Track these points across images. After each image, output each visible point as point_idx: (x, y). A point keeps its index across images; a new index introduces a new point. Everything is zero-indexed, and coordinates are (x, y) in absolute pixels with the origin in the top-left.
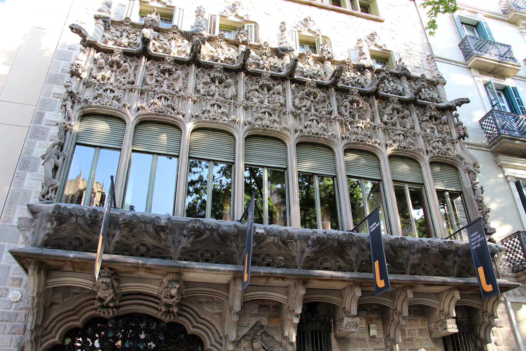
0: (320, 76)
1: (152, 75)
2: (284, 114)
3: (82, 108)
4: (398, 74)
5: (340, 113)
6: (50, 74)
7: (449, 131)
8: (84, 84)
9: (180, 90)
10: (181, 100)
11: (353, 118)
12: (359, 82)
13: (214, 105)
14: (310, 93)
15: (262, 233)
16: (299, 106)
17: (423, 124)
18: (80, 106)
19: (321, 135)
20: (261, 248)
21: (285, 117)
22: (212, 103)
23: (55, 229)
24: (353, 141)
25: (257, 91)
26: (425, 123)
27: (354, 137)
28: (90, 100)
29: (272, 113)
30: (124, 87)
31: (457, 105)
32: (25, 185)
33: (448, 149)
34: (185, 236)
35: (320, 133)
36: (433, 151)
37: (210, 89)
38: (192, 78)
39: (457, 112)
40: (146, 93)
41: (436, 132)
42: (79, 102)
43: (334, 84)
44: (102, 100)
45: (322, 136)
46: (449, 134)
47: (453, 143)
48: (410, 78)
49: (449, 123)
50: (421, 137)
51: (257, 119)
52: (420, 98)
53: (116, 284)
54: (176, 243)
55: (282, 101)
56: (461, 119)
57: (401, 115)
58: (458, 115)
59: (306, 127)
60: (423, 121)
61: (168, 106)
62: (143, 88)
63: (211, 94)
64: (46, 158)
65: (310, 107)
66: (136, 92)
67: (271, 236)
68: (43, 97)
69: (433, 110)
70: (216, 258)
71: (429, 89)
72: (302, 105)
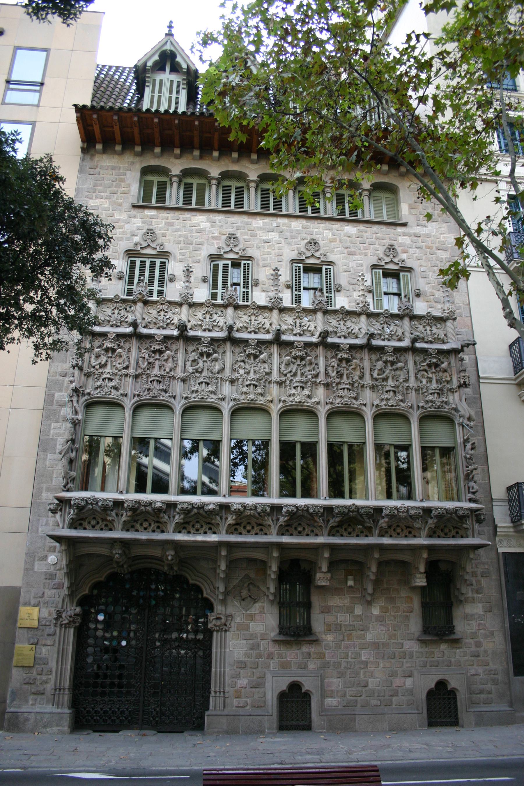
0: (310, 331)
1: (144, 358)
3: (86, 400)
5: (327, 374)
8: (85, 375)
9: (171, 370)
12: (353, 332)
16: (285, 373)
19: (304, 402)
20: (241, 519)
22: (200, 381)
23: (76, 514)
24: (337, 405)
25: (243, 361)
27: (338, 400)
30: (120, 373)
41: (434, 381)
50: (413, 391)
53: (127, 551)
54: (172, 518)
55: (267, 370)
60: (420, 370)
62: (137, 373)
63: (200, 370)
64: (63, 453)
70: (204, 528)
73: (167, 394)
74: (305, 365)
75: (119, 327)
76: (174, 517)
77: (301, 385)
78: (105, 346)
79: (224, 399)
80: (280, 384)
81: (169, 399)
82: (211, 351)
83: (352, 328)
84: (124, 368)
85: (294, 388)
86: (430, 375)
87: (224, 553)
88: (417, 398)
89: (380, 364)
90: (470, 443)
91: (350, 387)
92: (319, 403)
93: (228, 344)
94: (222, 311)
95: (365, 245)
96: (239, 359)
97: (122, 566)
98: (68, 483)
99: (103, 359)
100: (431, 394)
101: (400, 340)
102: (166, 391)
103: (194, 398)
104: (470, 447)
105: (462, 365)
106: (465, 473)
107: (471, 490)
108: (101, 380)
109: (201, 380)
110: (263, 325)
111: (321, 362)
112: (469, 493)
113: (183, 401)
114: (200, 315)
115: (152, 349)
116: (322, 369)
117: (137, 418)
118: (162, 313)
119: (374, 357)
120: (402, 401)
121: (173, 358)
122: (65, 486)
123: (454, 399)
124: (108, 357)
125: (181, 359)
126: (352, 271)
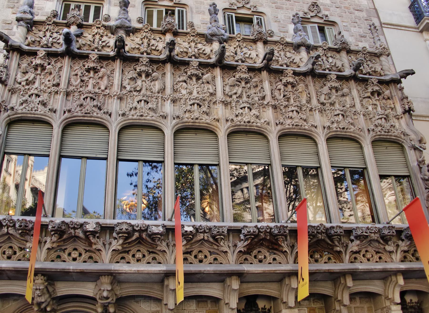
0: (252, 58)
1: (76, 75)
2: (214, 103)
3: (9, 116)
4: (336, 49)
5: (273, 98)
7: (393, 106)
8: (9, 91)
9: (106, 88)
10: (107, 98)
11: (288, 101)
12: (294, 61)
13: (141, 101)
14: (241, 79)
15: (191, 231)
16: (229, 94)
17: (365, 101)
18: (6, 114)
19: (253, 123)
21: (216, 107)
22: (138, 99)
24: (287, 126)
25: (185, 82)
26: (367, 99)
27: (289, 121)
28: (16, 108)
29: (201, 104)
30: (49, 90)
31: (402, 77)
33: (392, 125)
34: (115, 238)
35: (252, 121)
36: (375, 130)
37: (136, 85)
38: (117, 74)
39: (402, 85)
40: (72, 95)
41: (379, 108)
42: (5, 109)
43: (267, 68)
44: (28, 106)
45: (254, 124)
46: (394, 109)
47: (398, 119)
48: (349, 52)
49: (394, 97)
50: (362, 116)
51: (185, 112)
52: (362, 73)
54: (107, 246)
55: (211, 91)
56: (406, 92)
57: (340, 93)
58: (403, 88)
60: (364, 98)
61: (94, 106)
62: (68, 90)
63: (138, 89)
65: (242, 94)
66: (62, 94)
69: (375, 85)
70: (147, 258)
71: (371, 62)
72: (233, 92)
73: (102, 111)
74: (250, 88)
76: (110, 244)
77: (248, 106)
78: (34, 64)
79: (165, 117)
80: (226, 104)
84: (54, 85)
86: (375, 102)
91: (299, 110)
93: (168, 66)
94: (160, 38)
95: (290, 2)
99: (30, 76)
102: (100, 109)
103: (133, 116)
105: (403, 94)
109: (140, 98)
110: (203, 51)
111: (266, 85)
114: (138, 40)
116: (268, 92)
118: (97, 37)
119: (318, 85)
121: (109, 77)
124: (37, 75)
125: (117, 76)
126: (282, 22)
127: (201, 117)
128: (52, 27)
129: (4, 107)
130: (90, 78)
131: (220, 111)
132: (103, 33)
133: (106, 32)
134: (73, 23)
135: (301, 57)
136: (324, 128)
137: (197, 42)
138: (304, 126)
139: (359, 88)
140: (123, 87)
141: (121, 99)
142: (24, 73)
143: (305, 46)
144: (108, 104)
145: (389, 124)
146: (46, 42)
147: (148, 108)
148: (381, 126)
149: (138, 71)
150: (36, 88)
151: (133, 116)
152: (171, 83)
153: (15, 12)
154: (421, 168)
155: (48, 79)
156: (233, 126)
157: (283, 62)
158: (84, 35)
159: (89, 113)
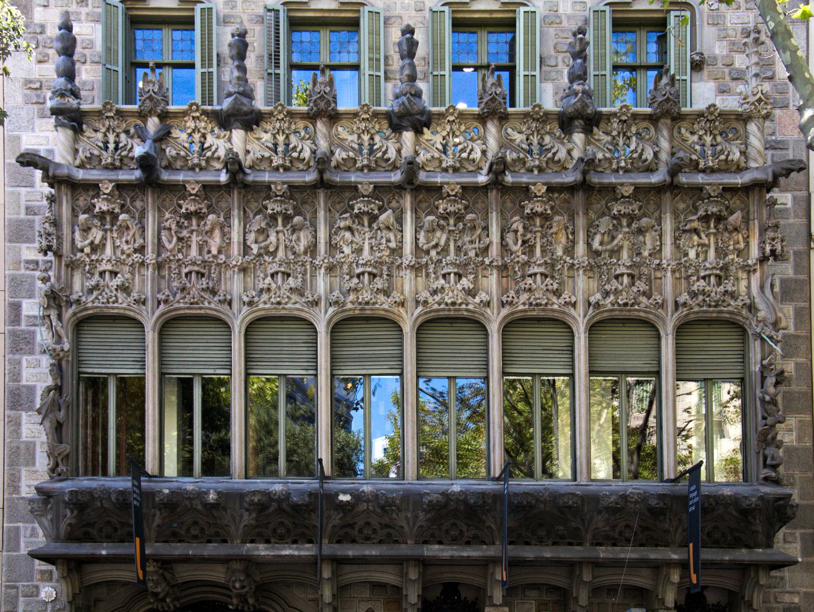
0: (474, 161)
3: (75, 314)
5: (504, 246)
6: (10, 220)
8: (67, 266)
9: (220, 252)
12: (556, 158)
16: (425, 247)
18: (71, 311)
19: (460, 304)
24: (521, 307)
25: (349, 229)
27: (524, 297)
30: (130, 261)
32: (24, 435)
35: (459, 301)
38: (236, 222)
40: (167, 266)
43: (496, 183)
44: (101, 294)
45: (464, 306)
49: (751, 222)
55: (393, 245)
59: (434, 292)
60: (685, 231)
62: (160, 259)
63: (271, 249)
67: (364, 501)
68: (11, 272)
73: (216, 298)
74: (462, 232)
75: (120, 168)
76: (241, 516)
77: (456, 270)
78: (97, 210)
79: (316, 303)
80: (417, 269)
81: (220, 307)
82: (290, 212)
83: (554, 151)
85: (444, 276)
87: (326, 573)
88: (674, 287)
89: (605, 224)
90: (773, 373)
92: (488, 304)
96: (342, 224)
97: (163, 600)
98: (57, 465)
99: (96, 235)
100: (704, 278)
101: (650, 170)
102: (214, 292)
103: (265, 303)
104: (774, 380)
106: (760, 429)
107: (768, 462)
108: (97, 276)
109: (274, 268)
112: (765, 466)
113: (245, 309)
115: (183, 210)
117: (171, 343)
120: (644, 293)
121: (222, 228)
122: (53, 470)
123: (749, 286)
127: (374, 300)
128: (116, 123)
129: (65, 299)
130: (192, 232)
131: (407, 283)
132: (205, 128)
133: (210, 126)
134: (150, 112)
135: (570, 146)
136: (590, 304)
137: (373, 131)
138: (553, 303)
139: (682, 206)
140: (246, 249)
141: (244, 270)
142: (84, 230)
143: (582, 118)
144: (225, 279)
145: (721, 289)
146: (109, 160)
147: (289, 287)
148: (704, 294)
149: (271, 212)
150: (109, 260)
151: (265, 303)
152: (325, 233)
153: (42, 59)
154: (763, 378)
155: (124, 239)
156: (426, 313)
157: (532, 164)
158: (174, 135)
159: (197, 303)
